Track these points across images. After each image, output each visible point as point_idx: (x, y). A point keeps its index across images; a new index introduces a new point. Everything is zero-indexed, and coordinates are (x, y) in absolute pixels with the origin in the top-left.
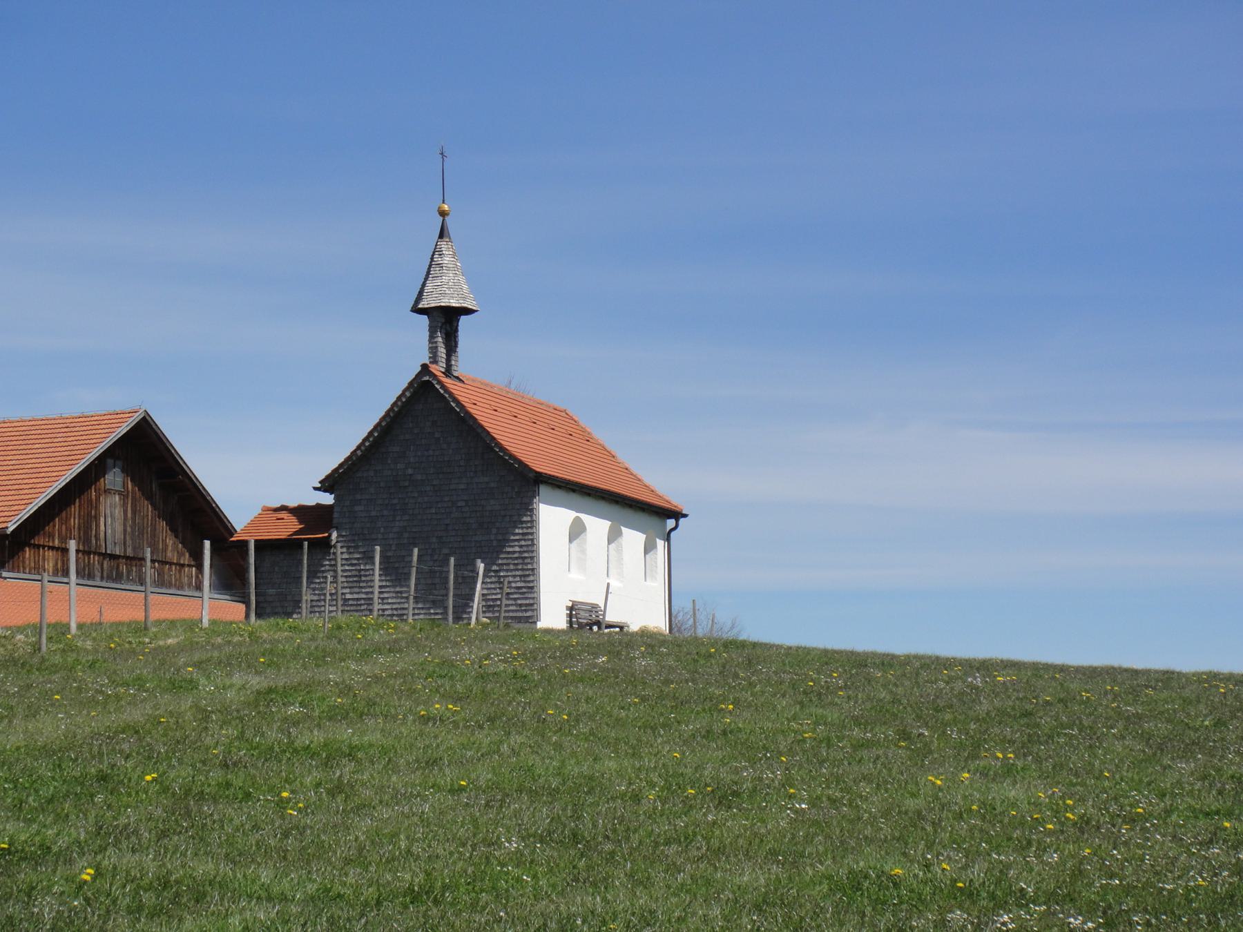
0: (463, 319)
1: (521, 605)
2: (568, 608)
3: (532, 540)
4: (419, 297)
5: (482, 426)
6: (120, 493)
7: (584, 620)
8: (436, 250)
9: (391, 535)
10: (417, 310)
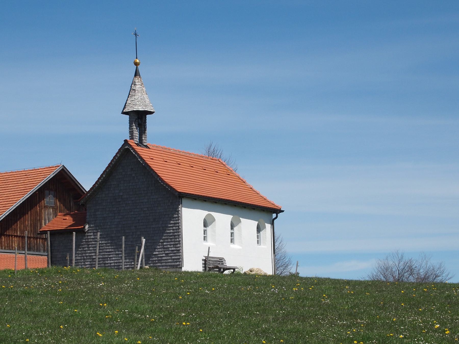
0: (148, 116)
1: (174, 259)
2: (203, 260)
3: (179, 226)
4: (125, 108)
5: (152, 170)
6: (53, 208)
7: (214, 266)
8: (134, 83)
9: (113, 226)
10: (123, 113)
